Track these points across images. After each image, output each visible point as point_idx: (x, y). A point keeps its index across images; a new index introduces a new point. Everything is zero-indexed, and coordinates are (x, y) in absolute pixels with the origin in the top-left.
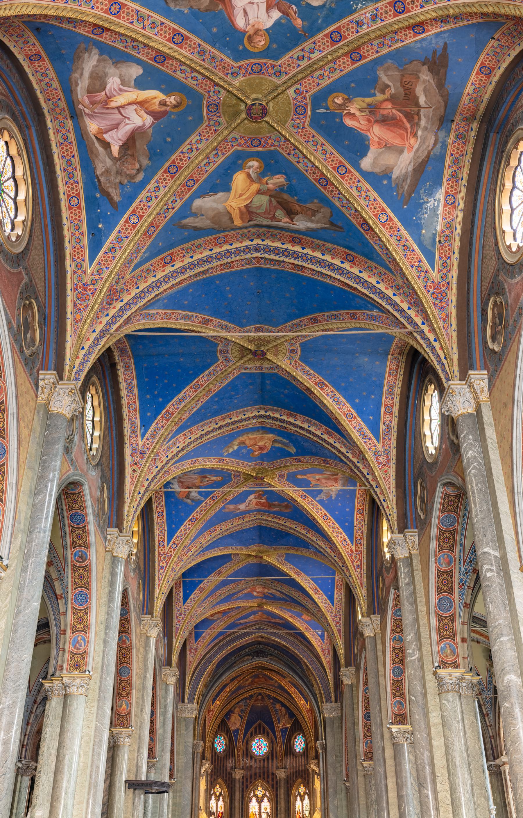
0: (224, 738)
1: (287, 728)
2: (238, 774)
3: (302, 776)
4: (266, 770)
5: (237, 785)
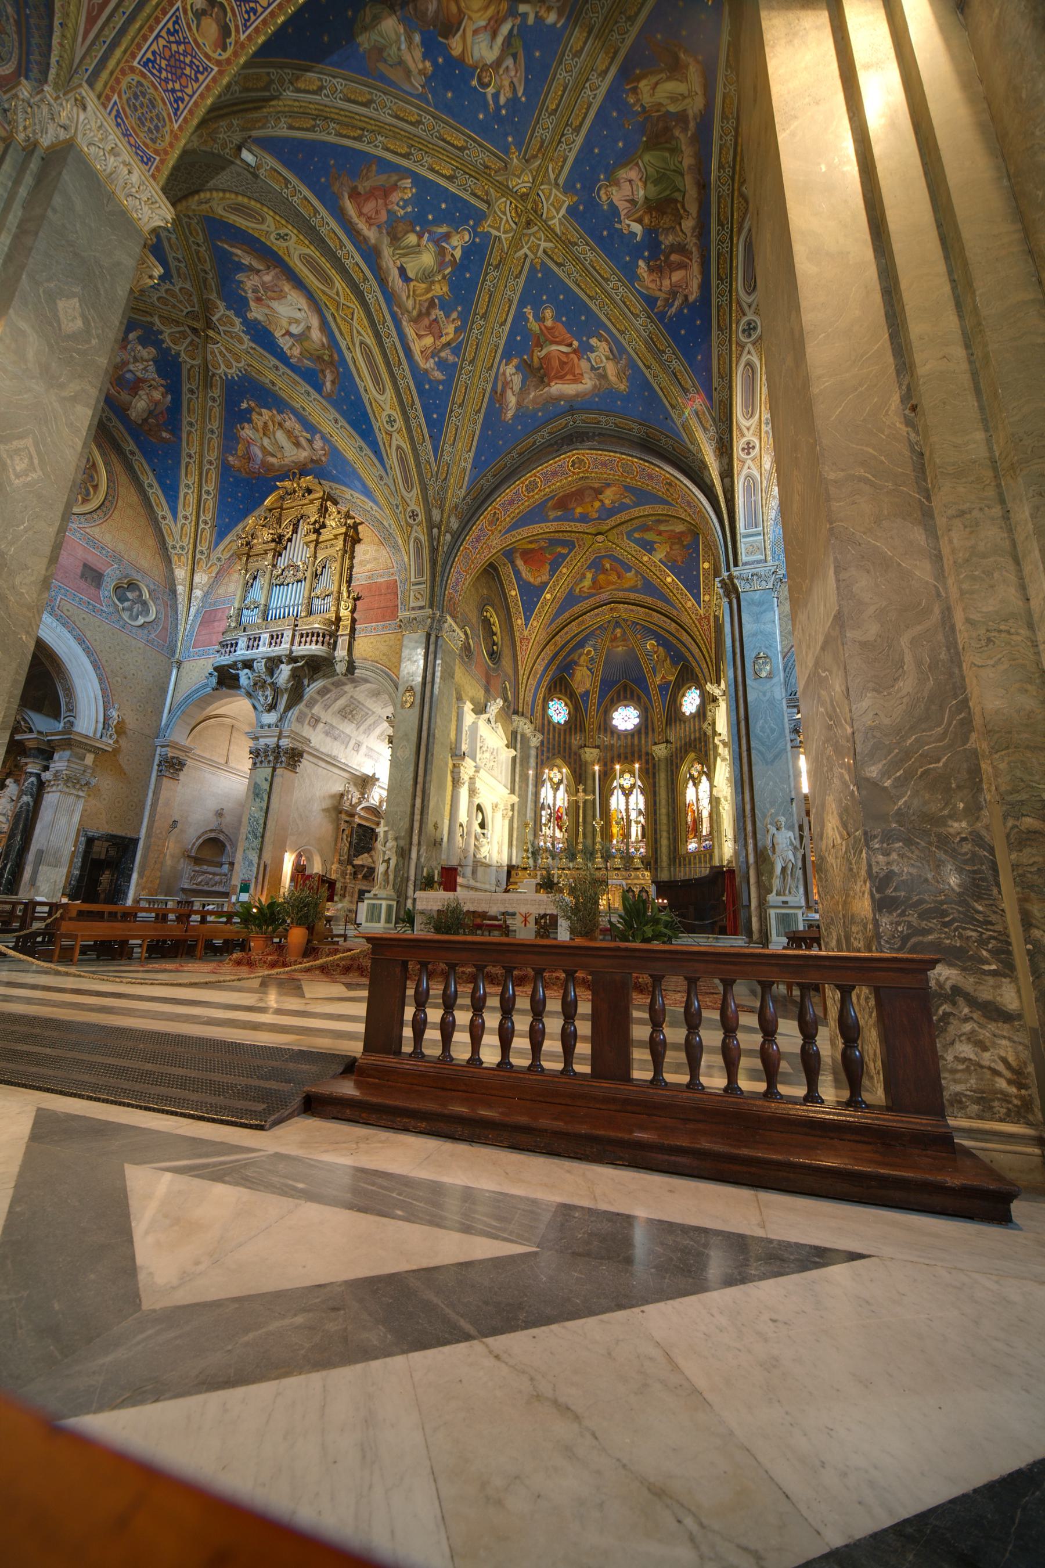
0: (566, 705)
1: (668, 683)
3: (695, 747)
4: (636, 749)
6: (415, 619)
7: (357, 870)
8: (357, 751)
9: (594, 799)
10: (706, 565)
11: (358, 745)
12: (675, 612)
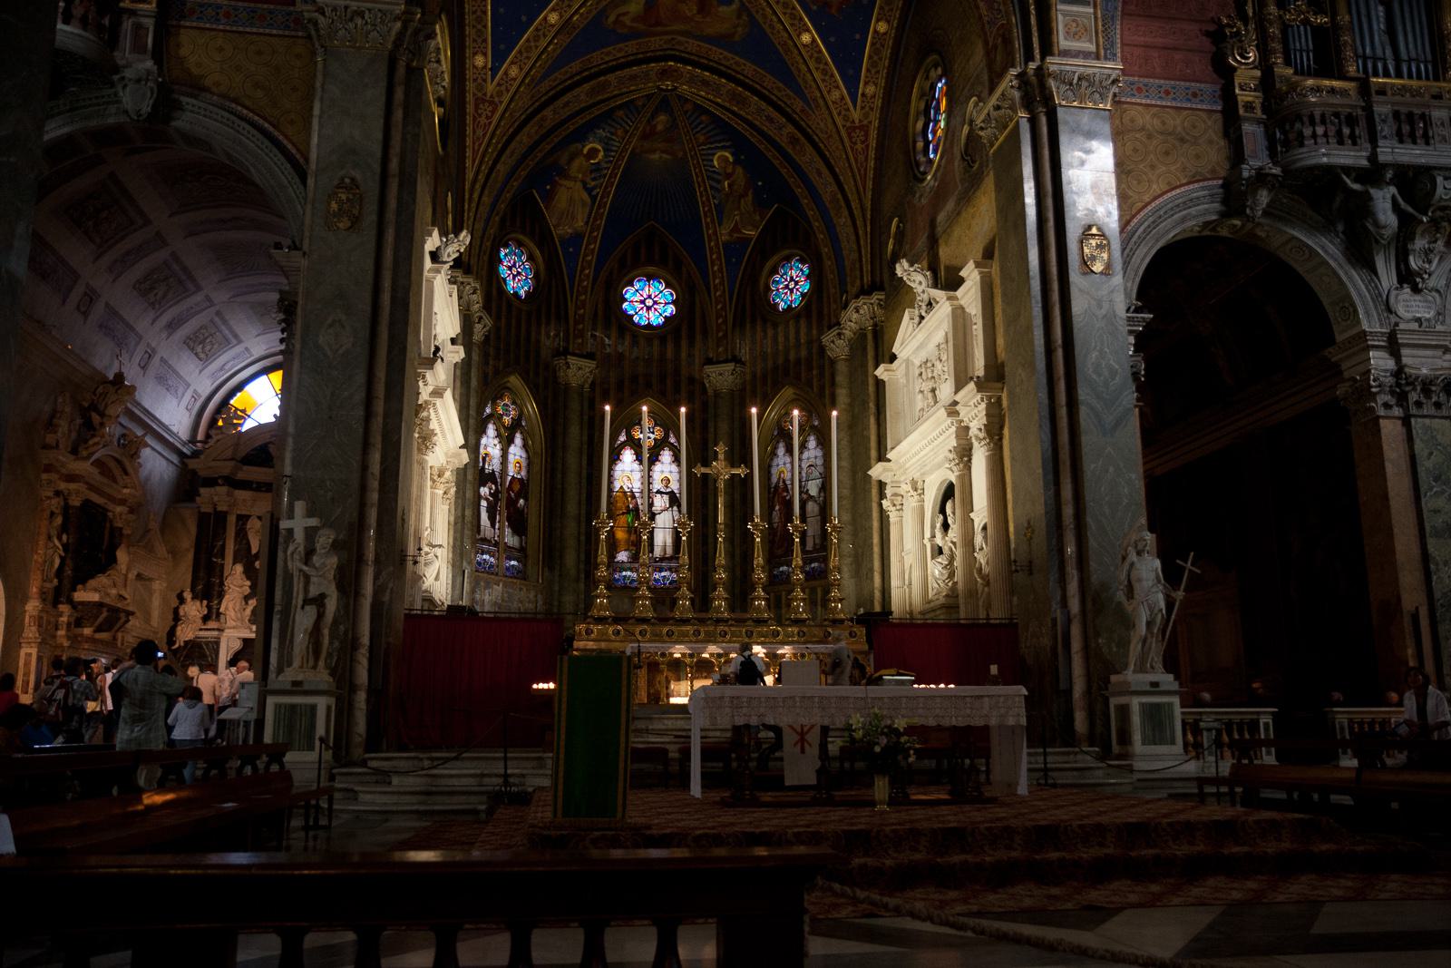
0: (531, 258)
1: (747, 240)
2: (578, 371)
5: (575, 405)
6: (361, 14)
7: (84, 614)
8: (85, 314)
9: (750, 476)
10: (882, 27)
11: (91, 297)
12: (798, 104)
